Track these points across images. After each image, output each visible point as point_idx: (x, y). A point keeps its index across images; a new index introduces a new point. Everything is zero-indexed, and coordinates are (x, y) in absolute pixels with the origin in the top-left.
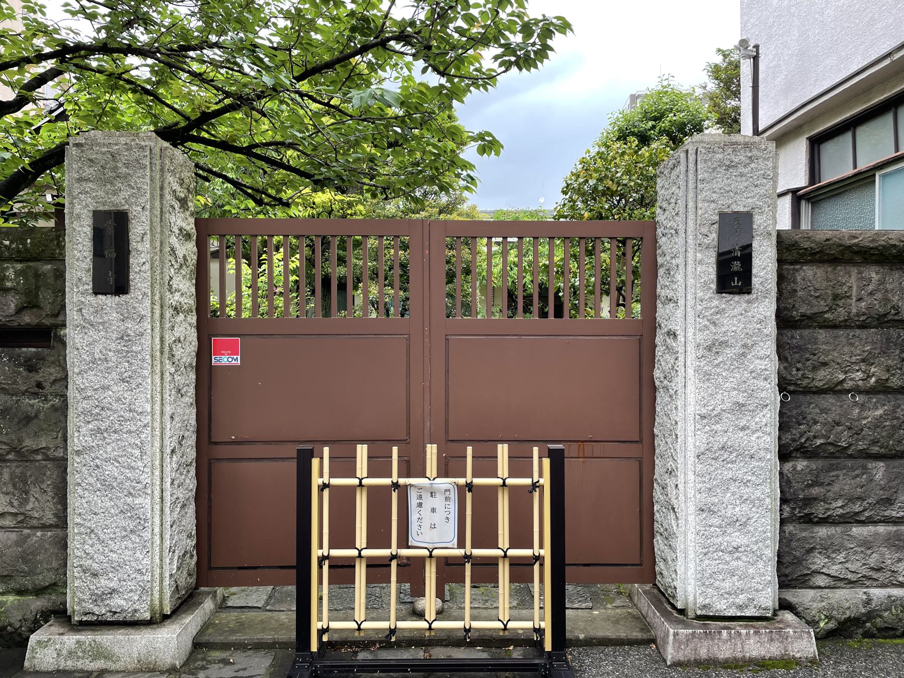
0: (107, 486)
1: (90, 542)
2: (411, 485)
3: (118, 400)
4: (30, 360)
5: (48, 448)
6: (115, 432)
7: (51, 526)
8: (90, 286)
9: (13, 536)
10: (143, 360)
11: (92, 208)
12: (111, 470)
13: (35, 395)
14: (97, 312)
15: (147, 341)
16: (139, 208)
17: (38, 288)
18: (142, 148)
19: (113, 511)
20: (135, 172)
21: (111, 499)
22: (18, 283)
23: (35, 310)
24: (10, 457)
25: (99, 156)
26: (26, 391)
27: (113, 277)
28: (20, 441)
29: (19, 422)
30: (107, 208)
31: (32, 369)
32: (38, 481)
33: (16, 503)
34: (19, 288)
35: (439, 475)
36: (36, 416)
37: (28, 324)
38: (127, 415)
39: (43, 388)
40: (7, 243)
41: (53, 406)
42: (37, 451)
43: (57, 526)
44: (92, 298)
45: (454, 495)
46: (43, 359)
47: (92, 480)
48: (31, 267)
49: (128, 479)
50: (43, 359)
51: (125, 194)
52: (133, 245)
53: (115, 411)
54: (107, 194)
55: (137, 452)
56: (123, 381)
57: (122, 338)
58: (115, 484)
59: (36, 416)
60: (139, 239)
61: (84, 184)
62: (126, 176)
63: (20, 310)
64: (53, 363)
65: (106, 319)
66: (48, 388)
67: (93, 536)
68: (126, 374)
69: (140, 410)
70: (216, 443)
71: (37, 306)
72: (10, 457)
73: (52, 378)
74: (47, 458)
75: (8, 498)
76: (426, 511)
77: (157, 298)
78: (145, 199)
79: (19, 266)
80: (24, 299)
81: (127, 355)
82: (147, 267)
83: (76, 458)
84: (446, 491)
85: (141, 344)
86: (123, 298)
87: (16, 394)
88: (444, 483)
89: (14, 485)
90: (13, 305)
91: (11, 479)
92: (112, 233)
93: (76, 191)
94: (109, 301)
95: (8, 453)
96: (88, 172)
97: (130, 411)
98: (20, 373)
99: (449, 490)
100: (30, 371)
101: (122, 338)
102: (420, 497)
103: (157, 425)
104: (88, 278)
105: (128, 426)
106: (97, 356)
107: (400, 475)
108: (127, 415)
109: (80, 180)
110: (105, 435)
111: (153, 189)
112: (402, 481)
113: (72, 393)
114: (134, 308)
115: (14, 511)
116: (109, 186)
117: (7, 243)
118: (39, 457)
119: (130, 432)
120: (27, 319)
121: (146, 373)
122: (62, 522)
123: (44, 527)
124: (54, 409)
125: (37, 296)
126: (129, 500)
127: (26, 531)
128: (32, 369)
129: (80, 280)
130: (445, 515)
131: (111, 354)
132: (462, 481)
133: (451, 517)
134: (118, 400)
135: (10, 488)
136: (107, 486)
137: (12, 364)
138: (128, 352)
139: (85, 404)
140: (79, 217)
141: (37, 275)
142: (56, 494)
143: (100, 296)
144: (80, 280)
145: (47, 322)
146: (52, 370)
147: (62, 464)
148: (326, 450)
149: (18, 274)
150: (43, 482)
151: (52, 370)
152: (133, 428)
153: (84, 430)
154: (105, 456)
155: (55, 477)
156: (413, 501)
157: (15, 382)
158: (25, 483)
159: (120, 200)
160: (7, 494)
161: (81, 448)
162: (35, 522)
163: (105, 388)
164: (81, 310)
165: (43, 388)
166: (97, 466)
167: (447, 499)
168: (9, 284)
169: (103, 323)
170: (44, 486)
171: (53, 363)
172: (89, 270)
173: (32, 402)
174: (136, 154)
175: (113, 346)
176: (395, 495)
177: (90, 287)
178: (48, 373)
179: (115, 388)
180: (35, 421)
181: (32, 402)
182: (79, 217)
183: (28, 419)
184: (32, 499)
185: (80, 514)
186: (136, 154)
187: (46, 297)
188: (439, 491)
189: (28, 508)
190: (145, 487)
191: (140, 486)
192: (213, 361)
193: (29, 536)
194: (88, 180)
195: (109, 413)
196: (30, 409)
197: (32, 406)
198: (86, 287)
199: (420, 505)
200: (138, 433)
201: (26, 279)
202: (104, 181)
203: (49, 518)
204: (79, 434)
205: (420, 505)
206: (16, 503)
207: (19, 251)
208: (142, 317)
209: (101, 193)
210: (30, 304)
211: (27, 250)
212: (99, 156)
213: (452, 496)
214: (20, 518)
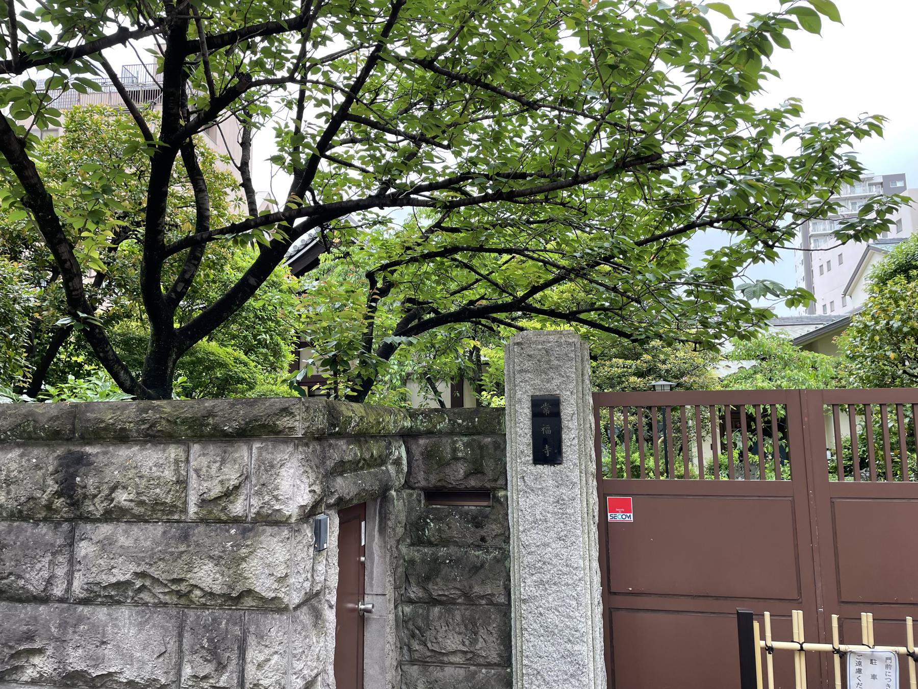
0: (549, 632)
1: (537, 683)
2: (851, 652)
3: (557, 556)
4: (476, 517)
5: (493, 595)
6: (555, 584)
7: (495, 664)
8: (531, 458)
9: (462, 672)
10: (576, 521)
11: (530, 394)
12: (552, 618)
13: (479, 547)
14: (536, 479)
15: (577, 504)
16: (568, 393)
17: (482, 457)
18: (570, 344)
19: (555, 656)
20: (565, 364)
21: (553, 645)
22: (467, 454)
23: (479, 475)
24: (460, 601)
25: (536, 352)
26: (472, 544)
27: (547, 450)
28: (471, 587)
29: (469, 571)
30: (542, 393)
31: (478, 525)
32: (486, 624)
33: (467, 643)
34: (469, 457)
35: (877, 643)
36: (482, 566)
37: (473, 487)
38: (565, 569)
39: (485, 542)
40: (460, 421)
41: (495, 557)
42: (482, 597)
43: (498, 665)
44: (532, 468)
45: (895, 663)
46: (487, 517)
47: (535, 626)
48: (475, 440)
49: (568, 627)
50: (487, 517)
51: (556, 382)
52: (565, 423)
53: (555, 566)
54: (542, 382)
55: (574, 603)
56: (560, 539)
57: (558, 502)
58: (556, 631)
59: (482, 566)
60: (569, 418)
61: (523, 374)
62: (557, 368)
63: (467, 476)
64: (495, 520)
65: (544, 485)
66: (490, 542)
67: (539, 677)
68: (562, 533)
69: (576, 565)
70: (615, 593)
71: (483, 473)
72: (460, 601)
73: (494, 533)
74: (491, 603)
75: (460, 637)
76: (865, 677)
77: (583, 467)
78: (571, 386)
79: (465, 439)
80: (471, 466)
81: (562, 516)
82: (576, 441)
83: (523, 606)
84: (887, 659)
85: (574, 508)
86: (558, 467)
87: (463, 546)
88: (885, 651)
89: (466, 626)
90: (462, 471)
91: (463, 621)
92: (546, 413)
93: (518, 381)
94: (545, 470)
95: (459, 597)
96: (527, 365)
97: (567, 566)
98: (468, 528)
99: (890, 659)
100: (477, 527)
101: (558, 502)
102: (860, 664)
103: (588, 579)
104: (529, 451)
105: (566, 579)
106: (538, 517)
107: (841, 642)
108: (565, 569)
109: (521, 371)
110: (547, 586)
111: (577, 376)
112: (843, 648)
113: (514, 546)
114: (567, 476)
115: (465, 649)
116: (544, 376)
117: (460, 421)
118: (484, 602)
119: (567, 585)
120: (473, 483)
121: (579, 532)
122: (506, 660)
123: (489, 665)
124: (497, 560)
125: (482, 465)
126: (569, 646)
127: (473, 668)
128: (478, 525)
129: (522, 452)
130: (886, 682)
131: (549, 515)
132: (902, 650)
133: (892, 684)
134: (557, 556)
135: (463, 629)
136: (549, 632)
137: (462, 521)
138: (563, 514)
139: (530, 559)
140: (520, 401)
141: (481, 447)
142: (500, 636)
143: (539, 466)
144: (522, 452)
145: (488, 485)
146: (494, 527)
147: (505, 610)
148: (767, 614)
149: (466, 445)
150: (489, 624)
151: (494, 527)
152: (570, 582)
153: (528, 581)
154: (547, 605)
155: (498, 620)
156: (852, 667)
157: (464, 536)
158: (475, 625)
159: (553, 386)
160: (460, 633)
161: (526, 597)
162: (481, 660)
163: (546, 545)
164: (523, 477)
165: (485, 542)
166: (541, 614)
167: (887, 666)
168: (460, 455)
169: (541, 489)
170: (490, 628)
171: (495, 520)
172: (529, 445)
173: (477, 553)
174: (565, 349)
175: (550, 509)
176: (837, 658)
177: (531, 458)
178: (493, 528)
179: (554, 545)
180: (482, 571)
181: (477, 553)
182: (520, 401)
183: (476, 569)
184: (481, 640)
185: (527, 657)
186: (565, 349)
187: (489, 465)
188: (880, 659)
189: (477, 647)
190: (582, 636)
191: (578, 634)
192: (609, 518)
193: (475, 673)
194: (527, 371)
195: (550, 567)
196: (476, 559)
197: (478, 557)
198: (528, 458)
199: (859, 671)
200: (575, 586)
201: (472, 450)
202: (539, 371)
203: (494, 657)
204: (524, 585)
205: (859, 671)
206: (467, 643)
207: (468, 428)
208: (574, 484)
209: (537, 381)
210: (477, 470)
211: (474, 427)
212: (536, 352)
213: (893, 664)
214: (469, 656)
